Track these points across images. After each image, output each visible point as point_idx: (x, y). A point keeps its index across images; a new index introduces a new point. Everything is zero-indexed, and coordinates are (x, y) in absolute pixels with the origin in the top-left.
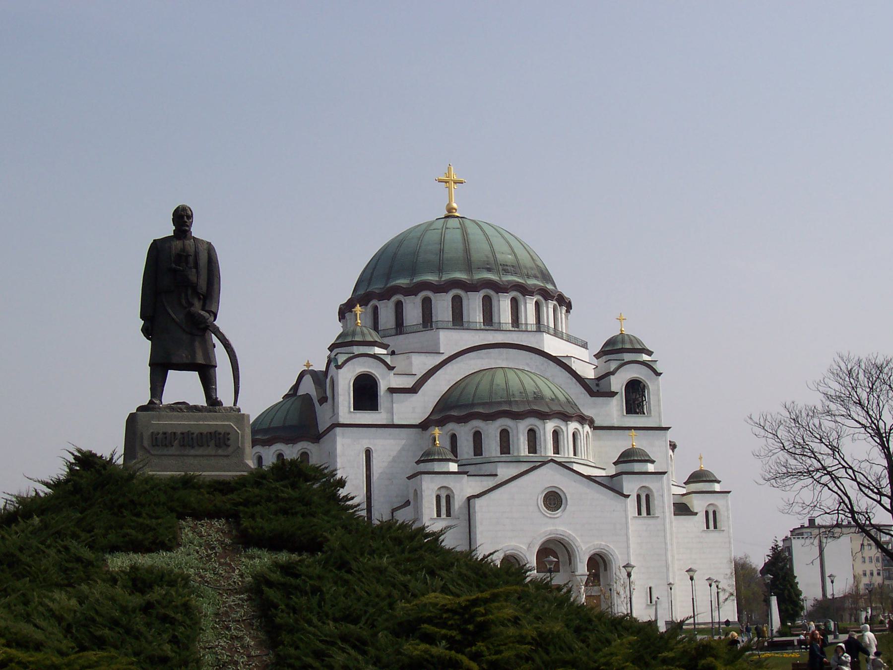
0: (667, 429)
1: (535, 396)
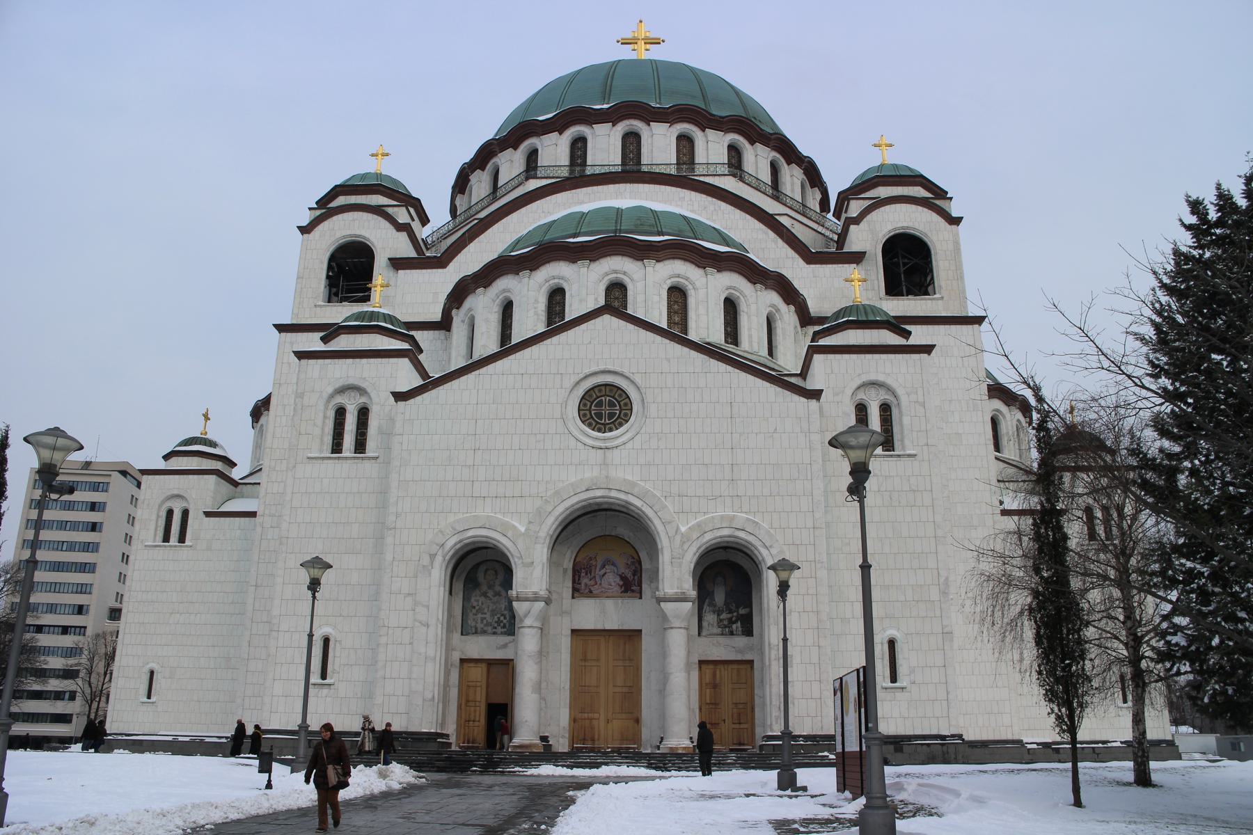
0: (979, 320)
1: (639, 222)
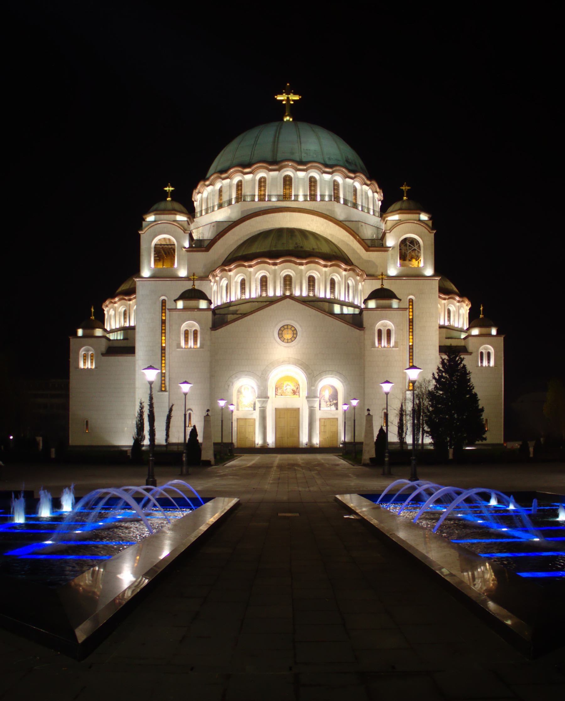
1: (296, 246)
